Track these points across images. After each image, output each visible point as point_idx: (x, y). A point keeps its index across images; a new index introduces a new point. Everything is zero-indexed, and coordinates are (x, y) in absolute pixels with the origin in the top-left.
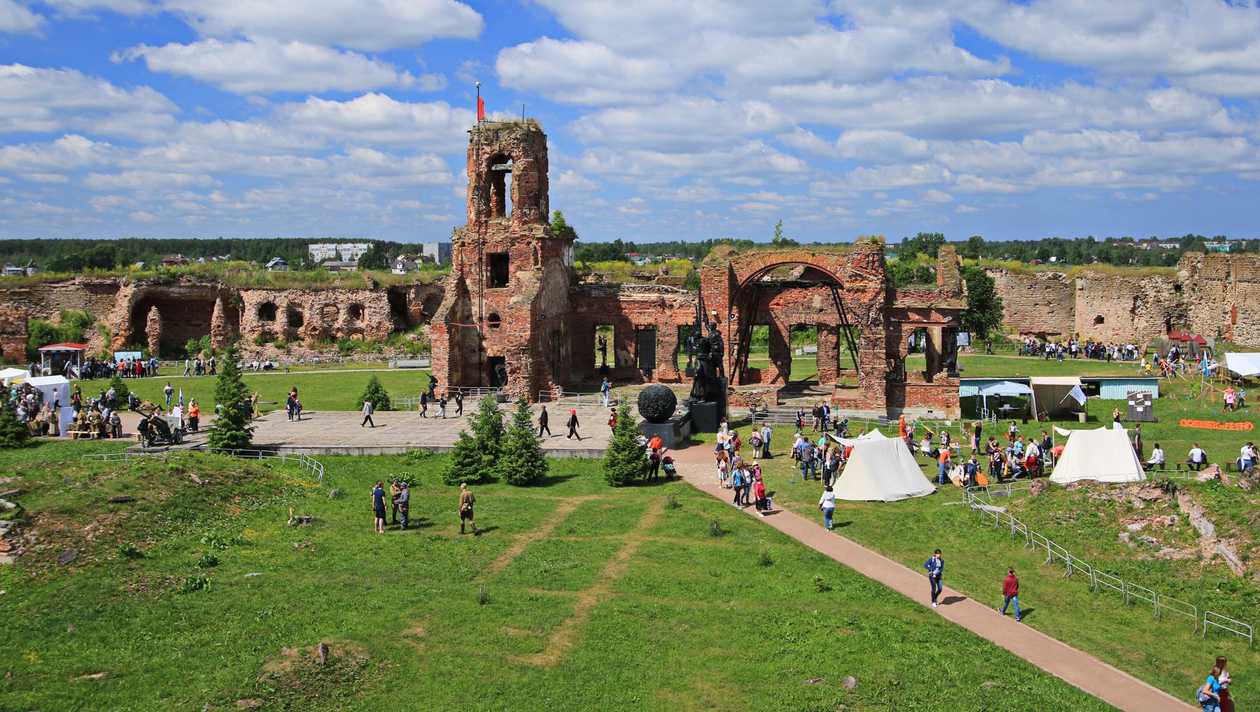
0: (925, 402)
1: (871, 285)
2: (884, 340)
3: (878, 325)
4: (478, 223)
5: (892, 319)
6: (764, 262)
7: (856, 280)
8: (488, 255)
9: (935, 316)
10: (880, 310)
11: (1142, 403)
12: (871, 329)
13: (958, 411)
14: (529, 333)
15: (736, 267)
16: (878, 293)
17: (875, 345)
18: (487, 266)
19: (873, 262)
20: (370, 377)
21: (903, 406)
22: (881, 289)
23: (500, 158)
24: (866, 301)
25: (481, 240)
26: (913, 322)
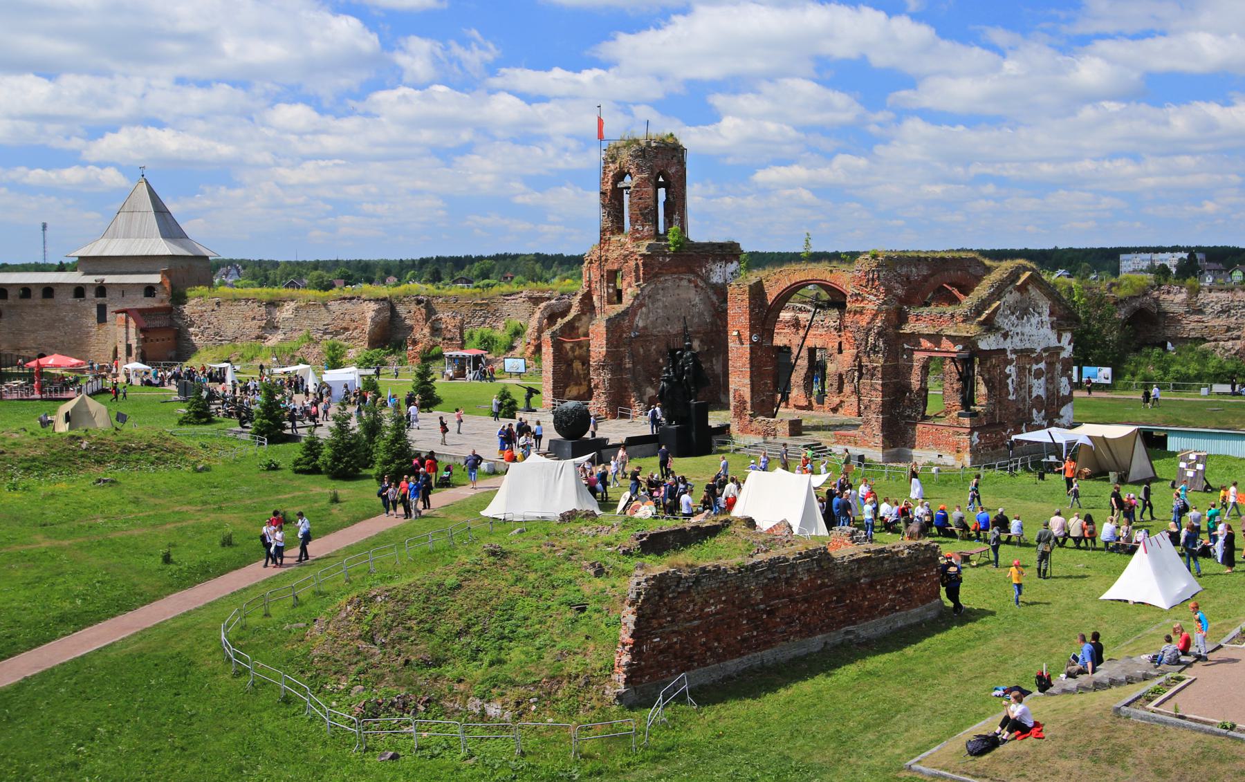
0: (937, 444)
1: (870, 306)
2: (880, 369)
3: (878, 352)
4: (603, 241)
5: (906, 346)
6: (790, 280)
7: (857, 300)
9: (946, 344)
10: (879, 334)
11: (1193, 466)
12: (869, 356)
13: (967, 459)
14: (605, 349)
15: (766, 285)
17: (873, 375)
18: (608, 282)
19: (873, 280)
20: (502, 386)
21: (913, 447)
23: (620, 176)
25: (603, 258)
26: (925, 350)
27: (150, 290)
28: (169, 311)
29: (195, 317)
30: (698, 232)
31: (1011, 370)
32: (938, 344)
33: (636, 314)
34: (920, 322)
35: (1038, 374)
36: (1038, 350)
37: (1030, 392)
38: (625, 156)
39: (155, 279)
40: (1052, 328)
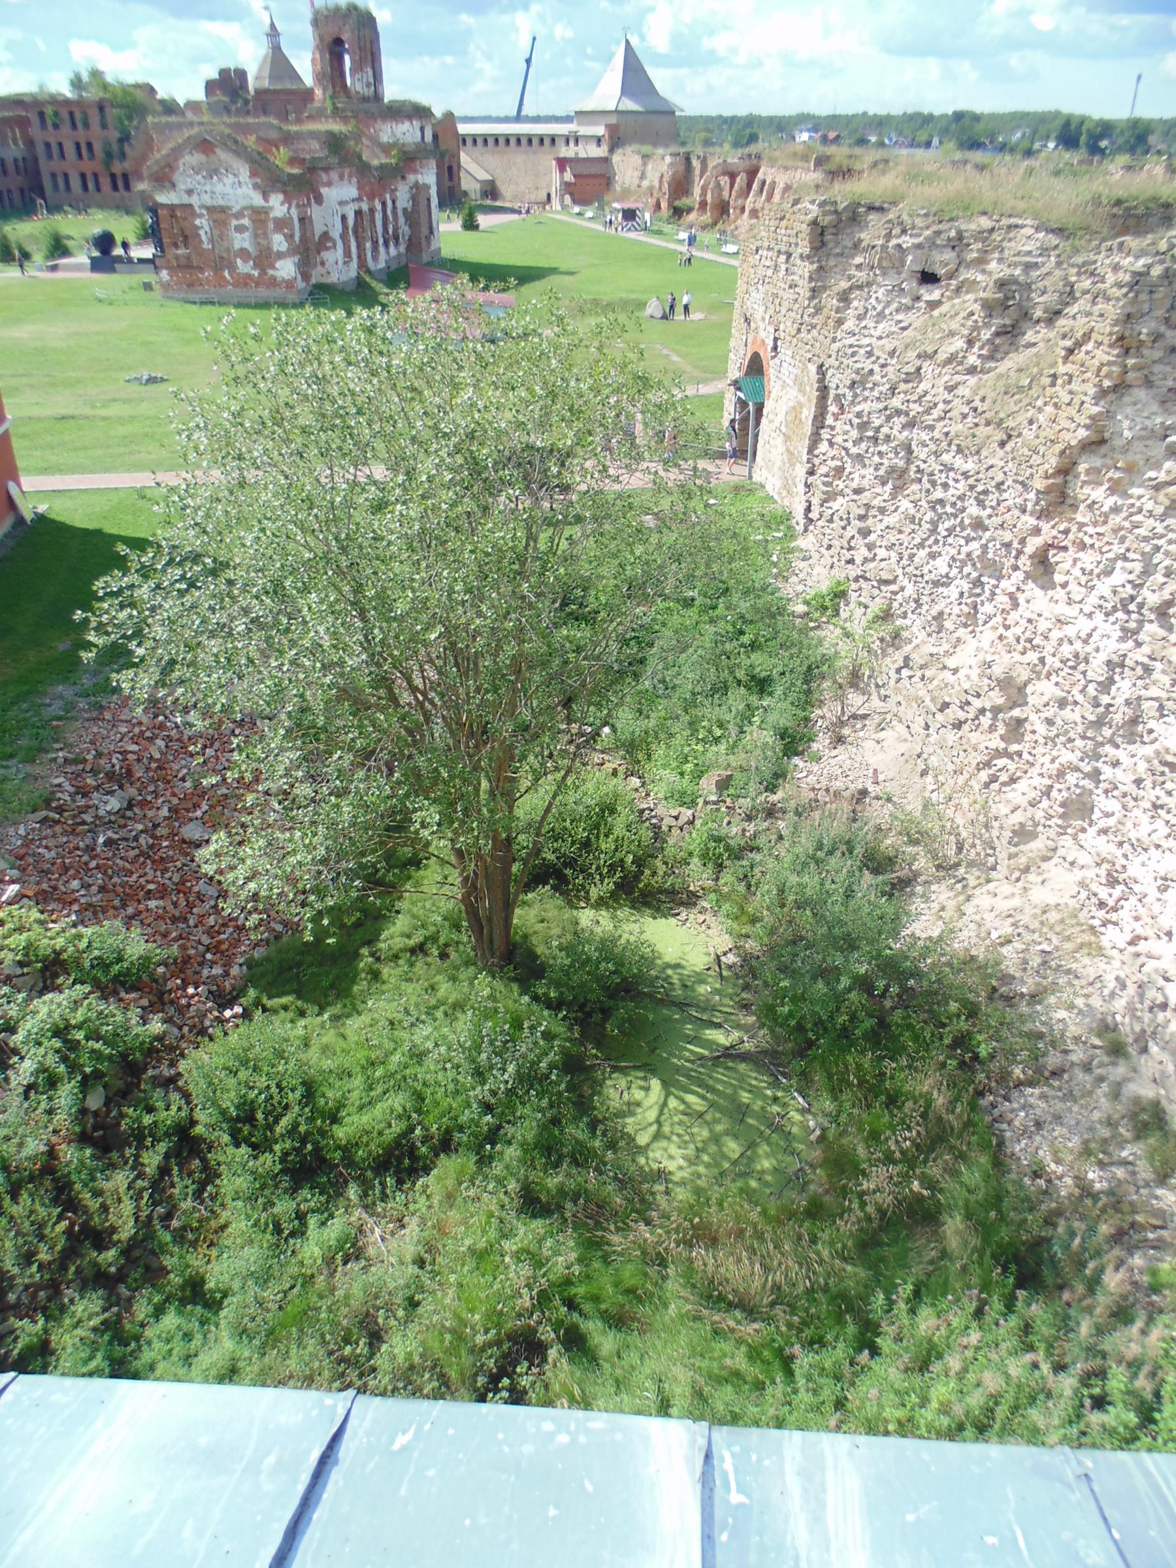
28: (606, 160)
35: (240, 229)
39: (600, 130)
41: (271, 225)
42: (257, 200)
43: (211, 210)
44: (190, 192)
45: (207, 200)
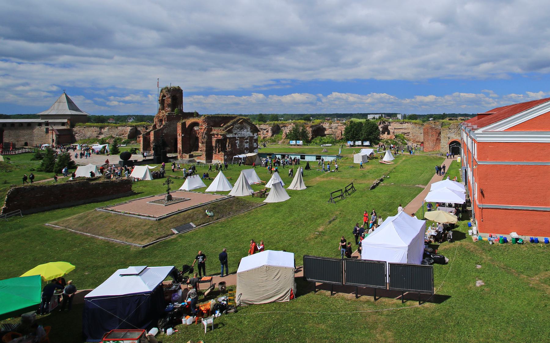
8: (160, 119)
10: (206, 134)
16: (204, 130)
18: (160, 122)
22: (205, 128)
24: (202, 132)
27: (63, 124)
29: (78, 131)
30: (186, 109)
31: (238, 142)
32: (218, 136)
33: (164, 130)
34: (215, 131)
35: (247, 142)
36: (247, 137)
37: (244, 146)
38: (164, 91)
39: (66, 121)
40: (251, 132)
41: (253, 141)
42: (251, 135)
43: (240, 138)
44: (236, 134)
45: (239, 135)
